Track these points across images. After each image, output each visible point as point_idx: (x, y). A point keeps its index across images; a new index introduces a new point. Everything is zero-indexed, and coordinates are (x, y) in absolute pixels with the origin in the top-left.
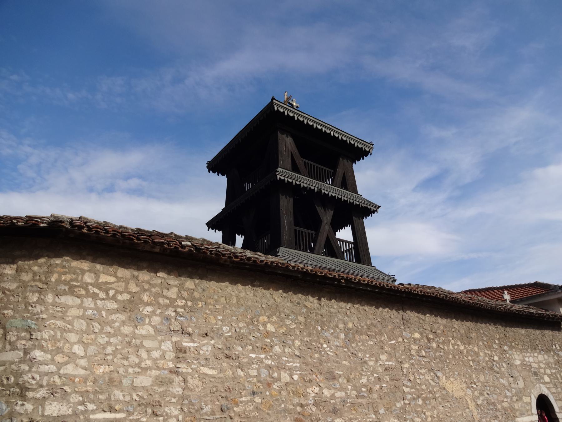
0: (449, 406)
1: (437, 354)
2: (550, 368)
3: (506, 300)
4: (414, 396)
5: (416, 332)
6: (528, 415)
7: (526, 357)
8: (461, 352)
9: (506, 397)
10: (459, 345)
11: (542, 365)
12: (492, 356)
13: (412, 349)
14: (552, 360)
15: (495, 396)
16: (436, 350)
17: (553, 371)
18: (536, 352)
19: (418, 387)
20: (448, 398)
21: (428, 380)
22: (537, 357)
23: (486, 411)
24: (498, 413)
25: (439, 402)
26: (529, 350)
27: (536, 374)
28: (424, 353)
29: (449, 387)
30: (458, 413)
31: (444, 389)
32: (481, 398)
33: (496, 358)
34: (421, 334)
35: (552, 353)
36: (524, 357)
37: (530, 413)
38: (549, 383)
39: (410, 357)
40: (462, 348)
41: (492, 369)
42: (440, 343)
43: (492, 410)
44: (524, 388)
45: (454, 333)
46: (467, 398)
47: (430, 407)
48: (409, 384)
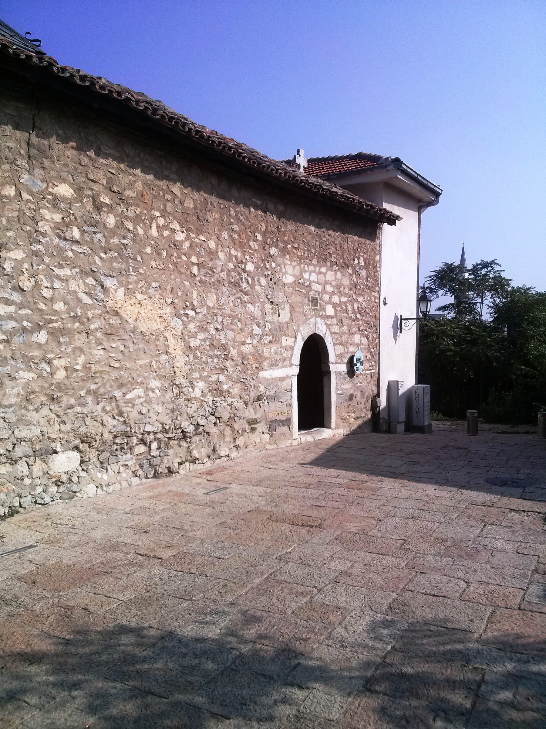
0: (122, 348)
1: (115, 241)
2: (340, 294)
3: (299, 166)
4: (25, 323)
5: (64, 181)
6: (285, 366)
7: (305, 271)
8: (176, 245)
9: (252, 335)
10: (174, 231)
11: (329, 288)
12: (242, 262)
13: (43, 219)
14: (346, 282)
15: (230, 334)
16: (113, 232)
17: (344, 299)
18: (326, 266)
19: (42, 306)
20: (121, 332)
21: (75, 292)
22: (325, 274)
23: (204, 359)
24: (228, 364)
25: (97, 339)
26: (314, 262)
27: (314, 301)
28: (76, 233)
29: (129, 311)
30: (140, 362)
31: (117, 313)
32: (201, 336)
33: (250, 267)
34: (79, 190)
35: (350, 271)
36: (302, 271)
37: (287, 363)
38: (332, 317)
39: (34, 237)
40: (180, 237)
41: (236, 285)
42: (127, 218)
43: (218, 357)
44: (287, 323)
45: (169, 204)
46: (167, 334)
47: (69, 350)
48: (16, 297)
